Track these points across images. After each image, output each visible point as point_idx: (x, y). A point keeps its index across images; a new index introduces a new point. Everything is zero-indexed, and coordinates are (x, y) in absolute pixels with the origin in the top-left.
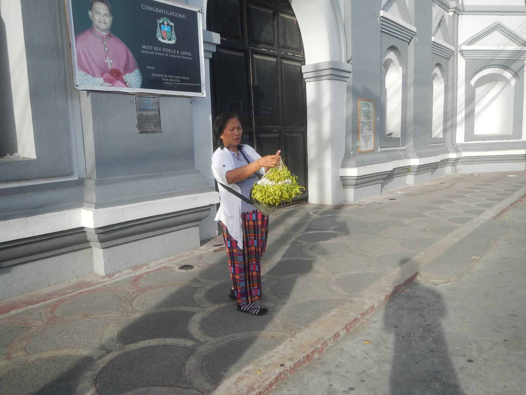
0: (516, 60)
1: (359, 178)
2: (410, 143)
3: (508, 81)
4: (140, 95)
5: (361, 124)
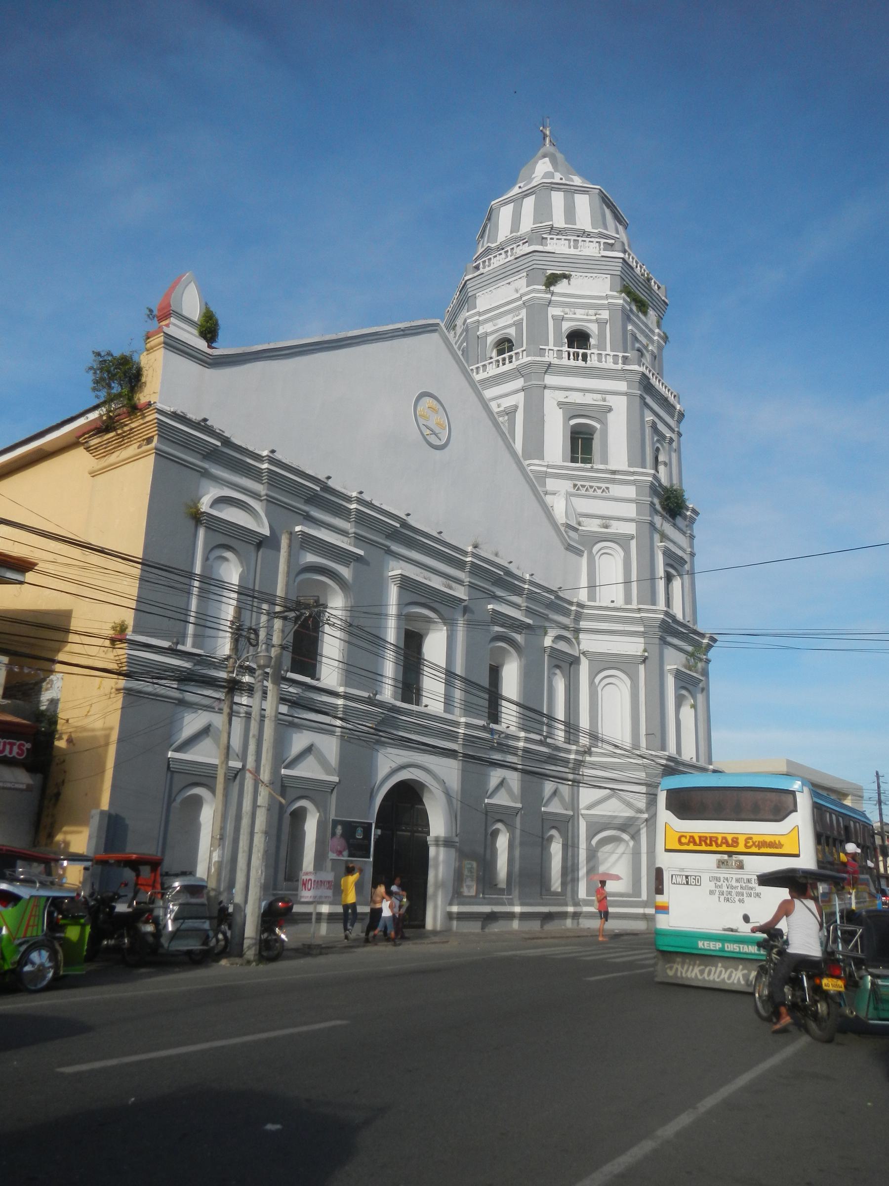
0: (632, 825)
1: (459, 913)
2: (516, 892)
3: (627, 843)
4: (347, 861)
5: (465, 877)
